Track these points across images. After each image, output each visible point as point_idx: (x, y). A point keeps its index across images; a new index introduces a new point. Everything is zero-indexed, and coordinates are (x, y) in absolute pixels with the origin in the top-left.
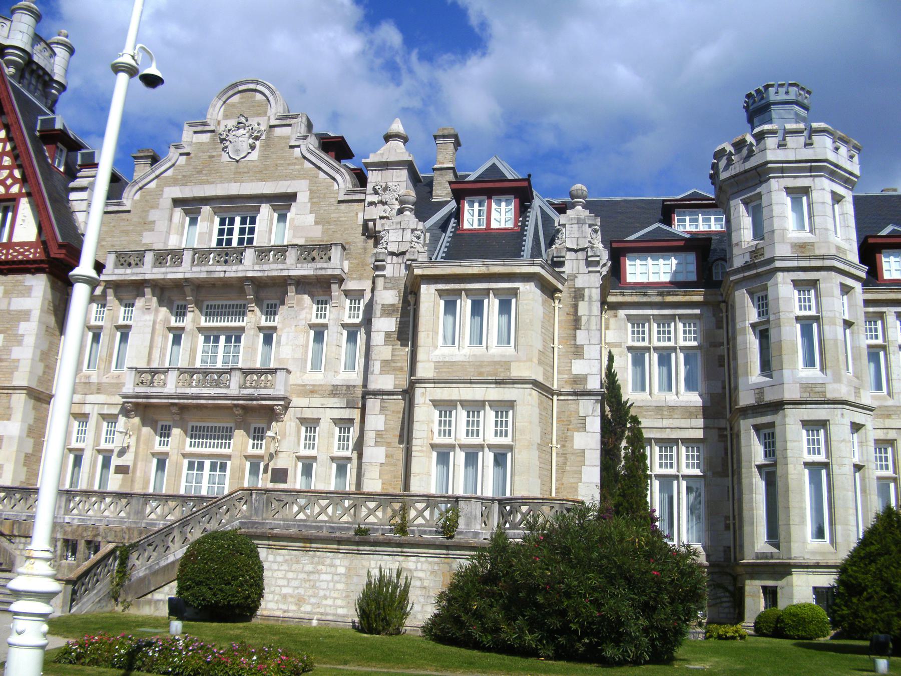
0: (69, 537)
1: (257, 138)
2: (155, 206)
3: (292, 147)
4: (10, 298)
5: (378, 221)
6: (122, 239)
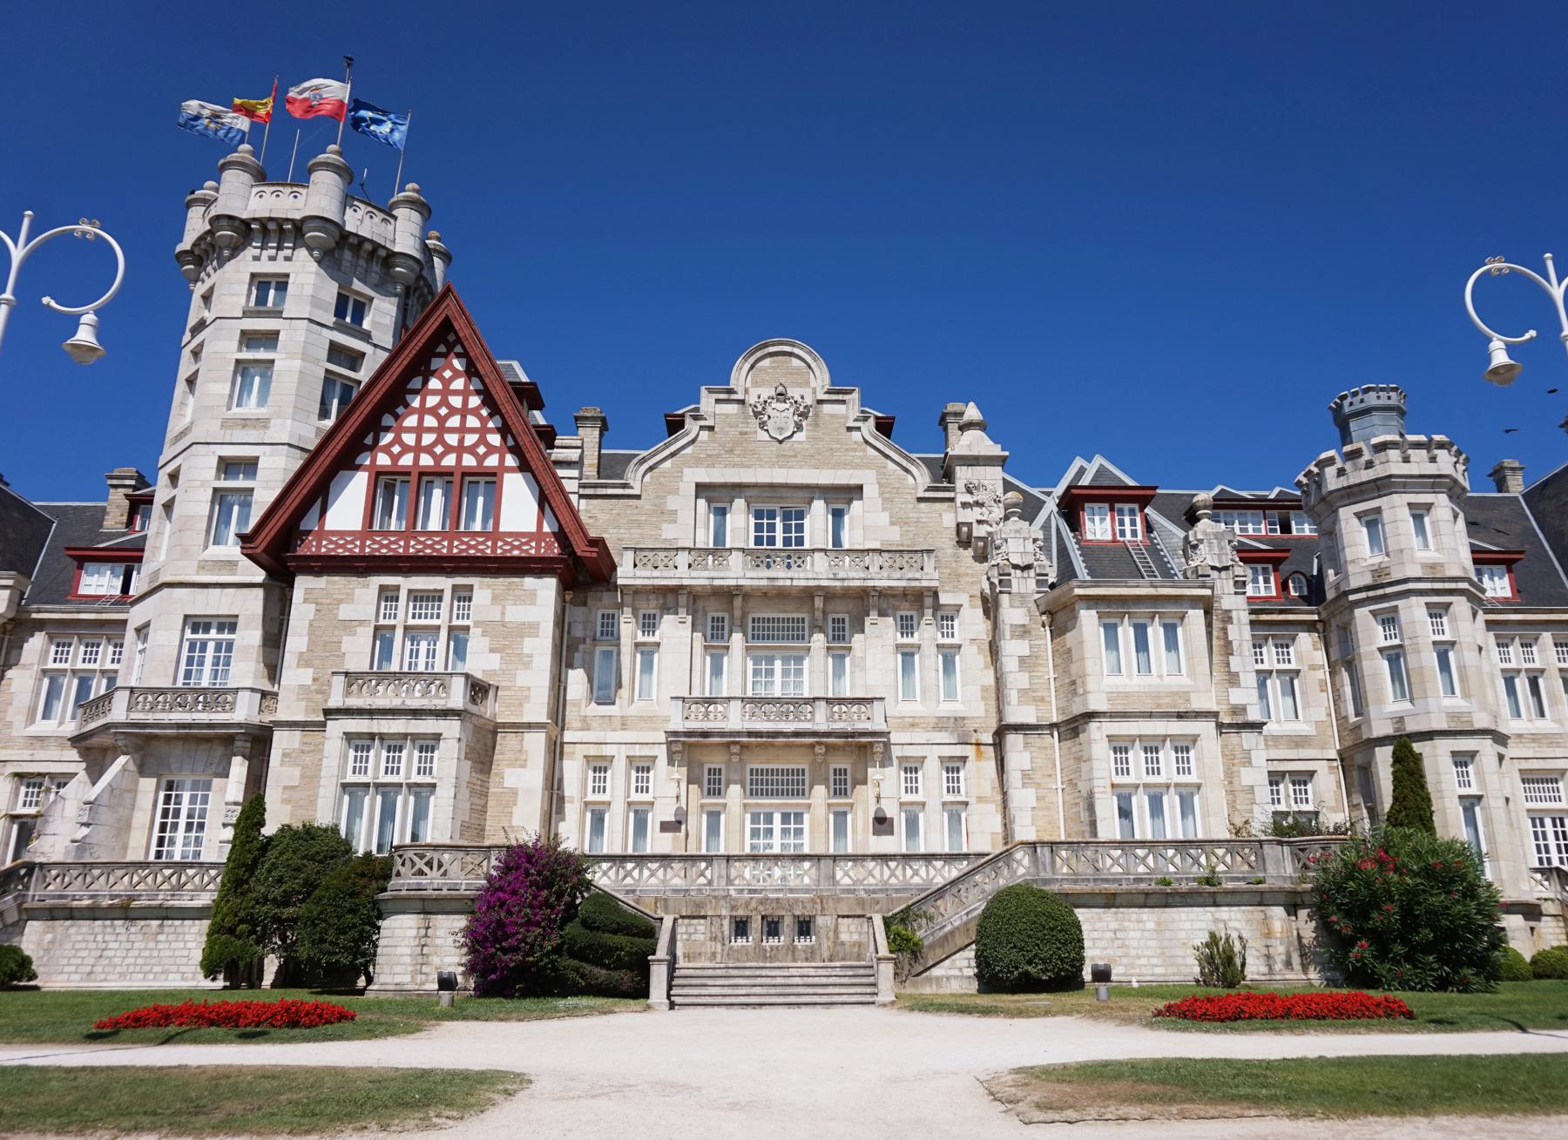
0: (741, 912)
1: (804, 415)
2: (676, 491)
3: (850, 429)
4: (504, 606)
5: (975, 525)
6: (633, 531)
